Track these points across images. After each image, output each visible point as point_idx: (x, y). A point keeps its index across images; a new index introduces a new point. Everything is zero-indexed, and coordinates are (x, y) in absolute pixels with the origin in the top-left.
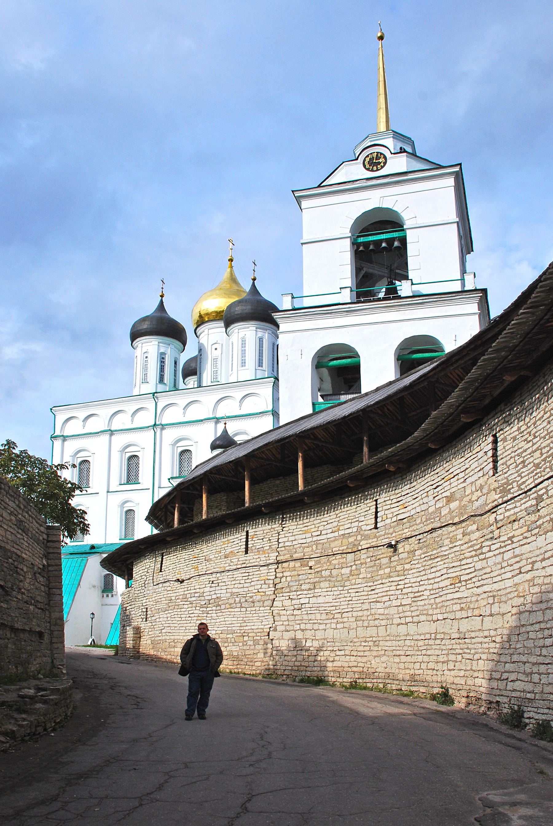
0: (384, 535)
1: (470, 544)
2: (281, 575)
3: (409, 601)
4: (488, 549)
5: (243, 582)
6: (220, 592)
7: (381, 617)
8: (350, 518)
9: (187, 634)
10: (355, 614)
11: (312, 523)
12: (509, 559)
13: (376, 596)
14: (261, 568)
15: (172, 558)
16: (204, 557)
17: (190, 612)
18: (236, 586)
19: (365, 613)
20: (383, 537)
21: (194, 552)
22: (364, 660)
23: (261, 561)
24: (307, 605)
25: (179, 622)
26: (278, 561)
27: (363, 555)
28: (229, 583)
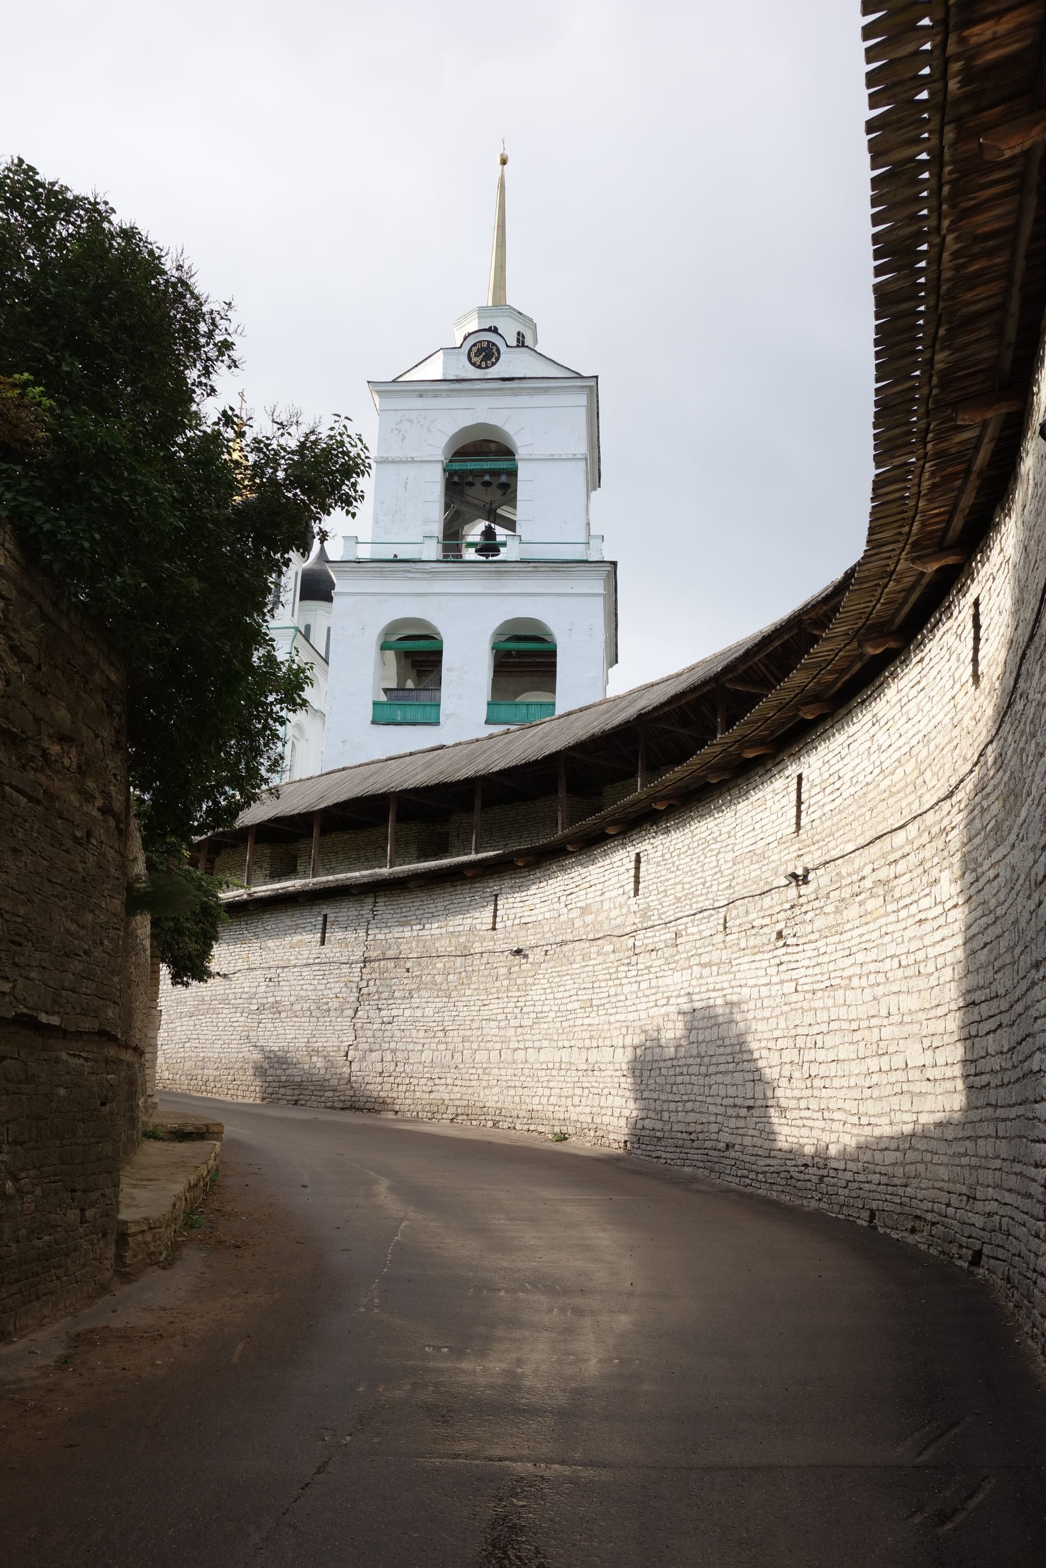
1: (604, 966)
2: (369, 977)
4: (624, 974)
10: (462, 1033)
11: (413, 913)
12: (646, 989)
14: (342, 966)
17: (232, 1020)
18: (304, 987)
19: (475, 1032)
20: (501, 942)
22: (470, 1090)
25: (214, 1033)
28: (295, 983)
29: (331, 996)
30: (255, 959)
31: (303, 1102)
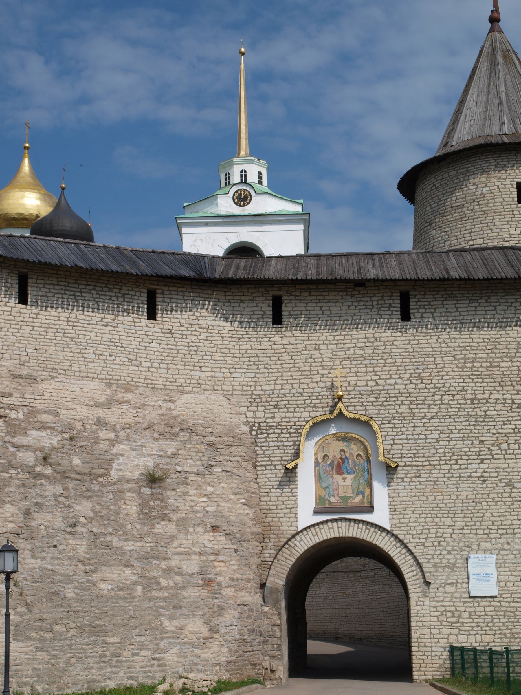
3: (322, 600)
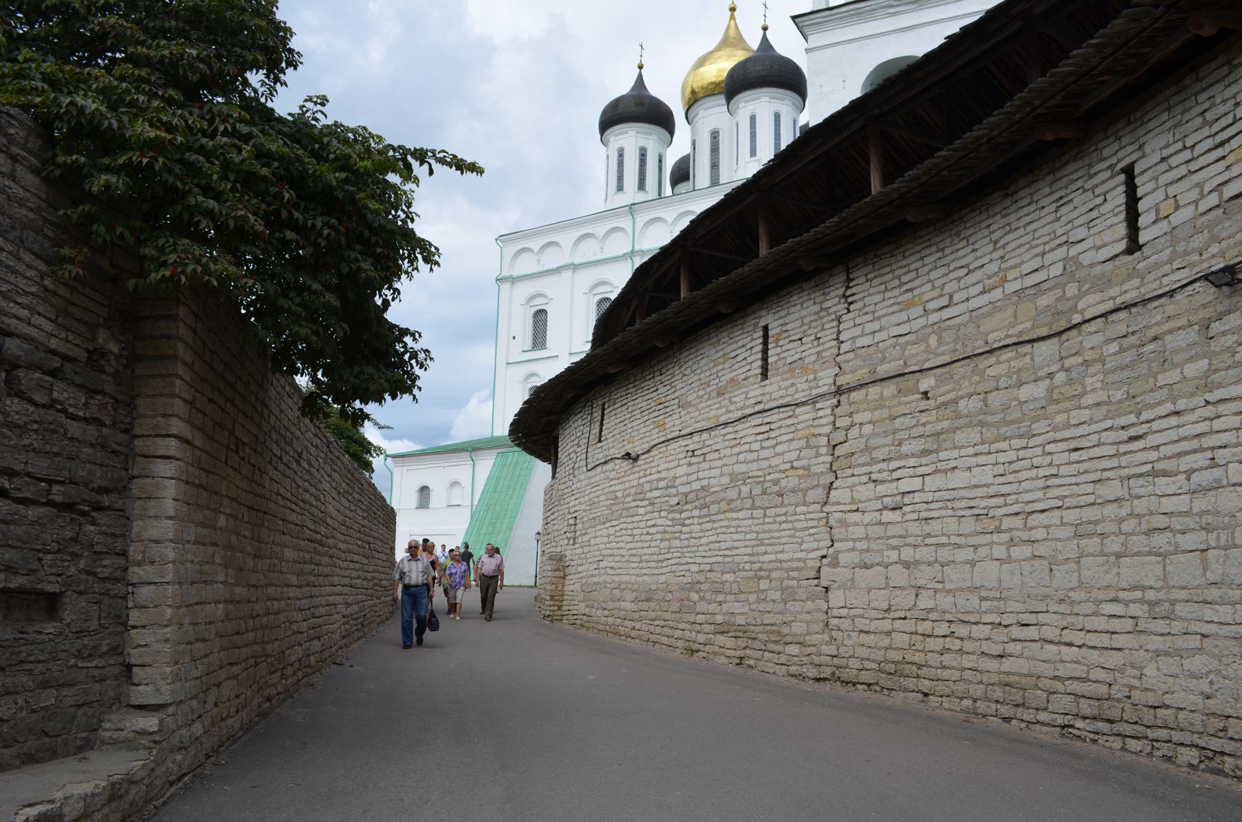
0: (1170, 261)
2: (847, 421)
5: (756, 446)
6: (707, 474)
7: (1176, 523)
8: (1039, 242)
9: (644, 571)
10: (1071, 516)
11: (925, 279)
13: (1153, 455)
14: (798, 410)
15: (619, 410)
16: (676, 401)
18: (742, 457)
19: (1110, 510)
20: (1167, 268)
21: (659, 392)
22: (1115, 659)
23: (797, 392)
24: (918, 497)
25: (629, 546)
26: (839, 387)
27: (1090, 338)
28: (728, 452)
29: (783, 467)
30: (674, 425)
31: (752, 662)
